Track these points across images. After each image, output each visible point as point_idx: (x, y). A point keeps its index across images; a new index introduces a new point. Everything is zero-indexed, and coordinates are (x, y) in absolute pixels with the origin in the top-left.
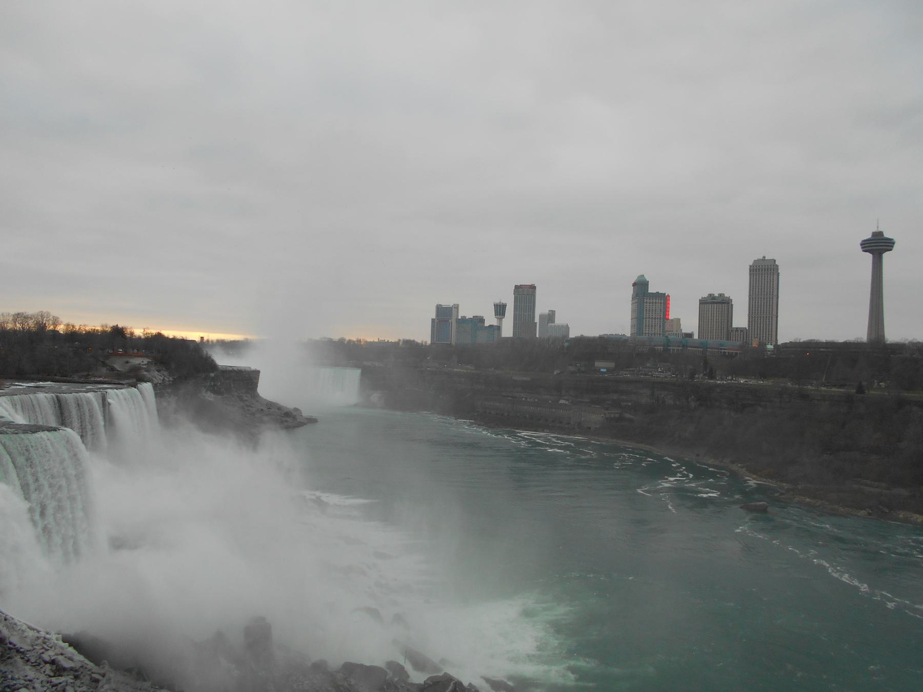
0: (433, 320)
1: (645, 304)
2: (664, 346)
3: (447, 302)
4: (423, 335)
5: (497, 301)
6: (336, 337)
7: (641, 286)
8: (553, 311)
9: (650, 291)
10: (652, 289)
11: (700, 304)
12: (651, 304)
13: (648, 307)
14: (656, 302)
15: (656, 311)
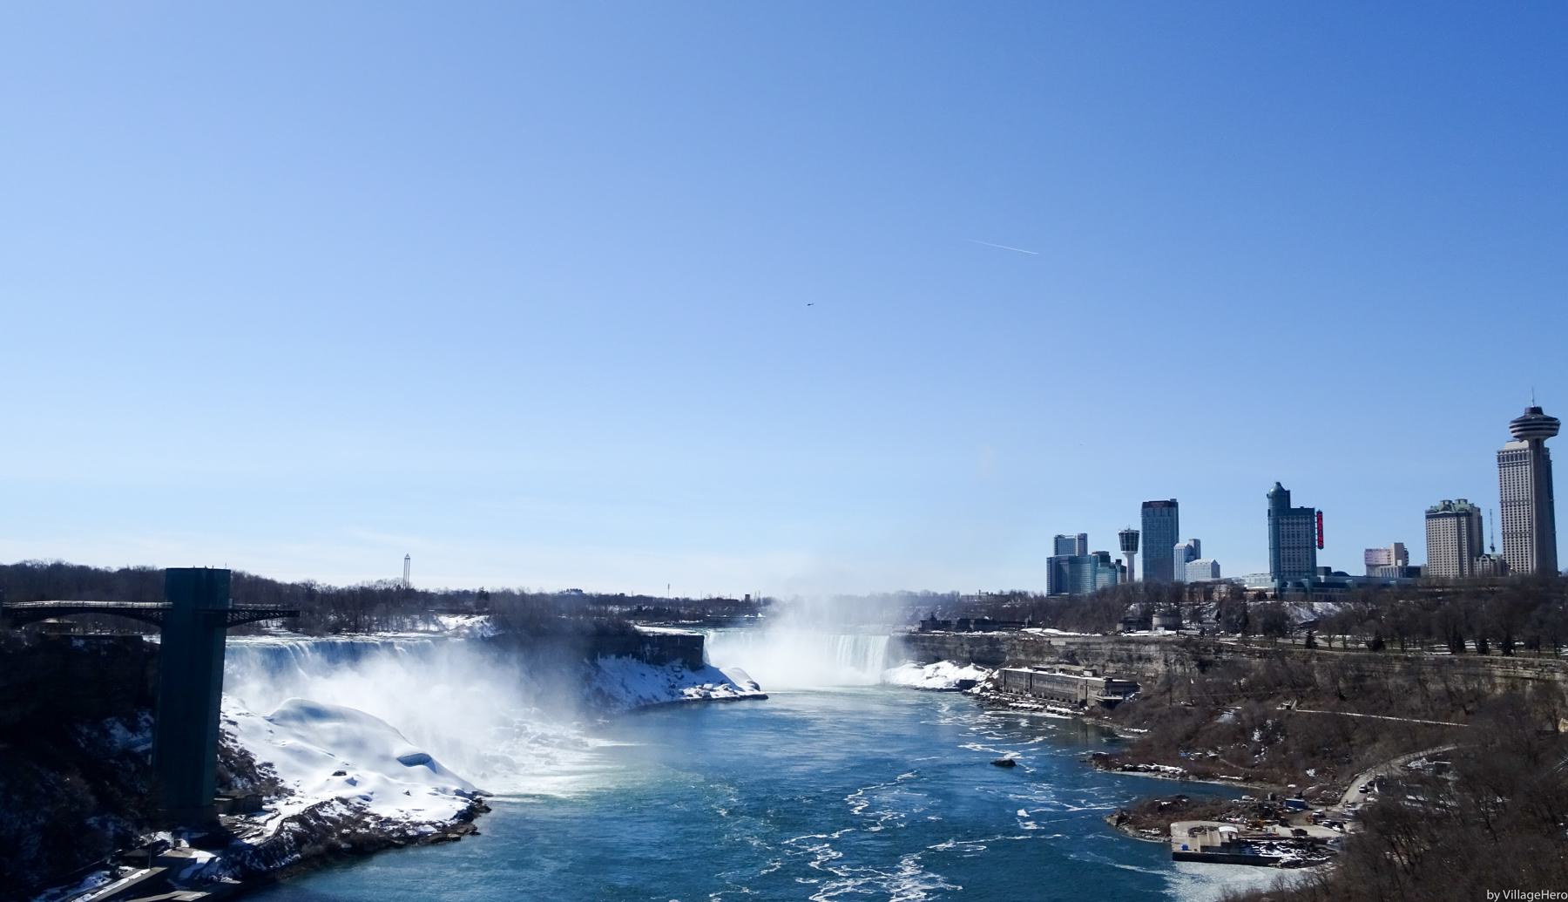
0: (1050, 560)
1: (1281, 527)
2: (1275, 589)
3: (1071, 532)
4: (1037, 585)
5: (1123, 528)
6: (918, 589)
7: (1280, 497)
8: (1195, 540)
9: (1292, 507)
10: (1295, 504)
11: (1428, 517)
12: (1290, 526)
13: (1285, 530)
14: (1298, 523)
15: (1298, 535)
